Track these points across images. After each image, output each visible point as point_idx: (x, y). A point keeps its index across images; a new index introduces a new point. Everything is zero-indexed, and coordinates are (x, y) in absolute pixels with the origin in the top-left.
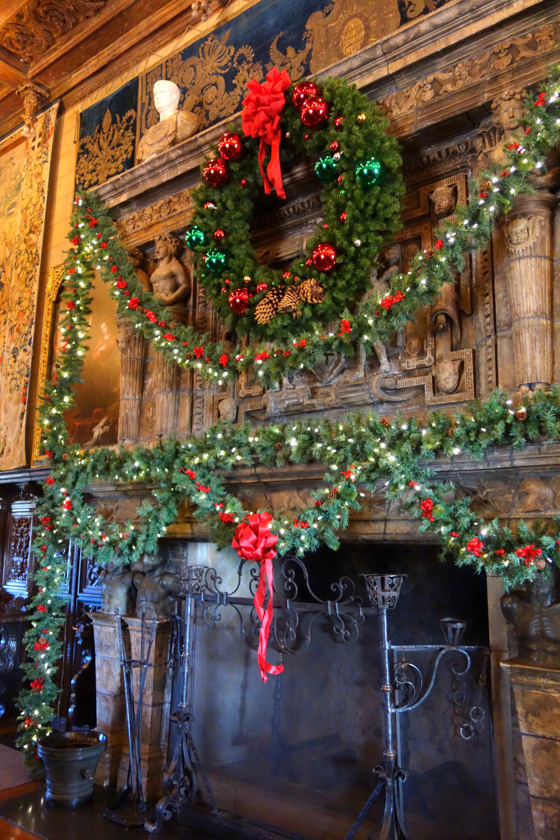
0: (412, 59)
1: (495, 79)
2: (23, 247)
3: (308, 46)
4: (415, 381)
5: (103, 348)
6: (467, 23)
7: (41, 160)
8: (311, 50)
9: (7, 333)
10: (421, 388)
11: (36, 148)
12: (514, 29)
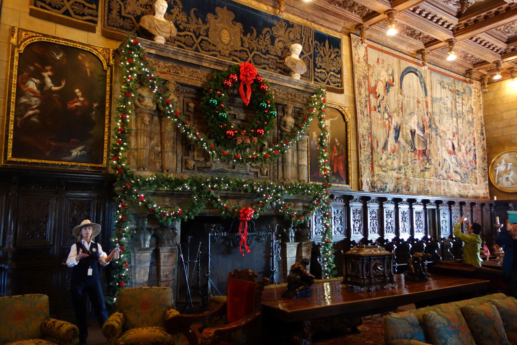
0: (274, 82)
1: (288, 100)
3: (208, 25)
4: (256, 170)
5: (78, 104)
6: (287, 83)
8: (209, 28)
10: (257, 173)
12: (292, 90)
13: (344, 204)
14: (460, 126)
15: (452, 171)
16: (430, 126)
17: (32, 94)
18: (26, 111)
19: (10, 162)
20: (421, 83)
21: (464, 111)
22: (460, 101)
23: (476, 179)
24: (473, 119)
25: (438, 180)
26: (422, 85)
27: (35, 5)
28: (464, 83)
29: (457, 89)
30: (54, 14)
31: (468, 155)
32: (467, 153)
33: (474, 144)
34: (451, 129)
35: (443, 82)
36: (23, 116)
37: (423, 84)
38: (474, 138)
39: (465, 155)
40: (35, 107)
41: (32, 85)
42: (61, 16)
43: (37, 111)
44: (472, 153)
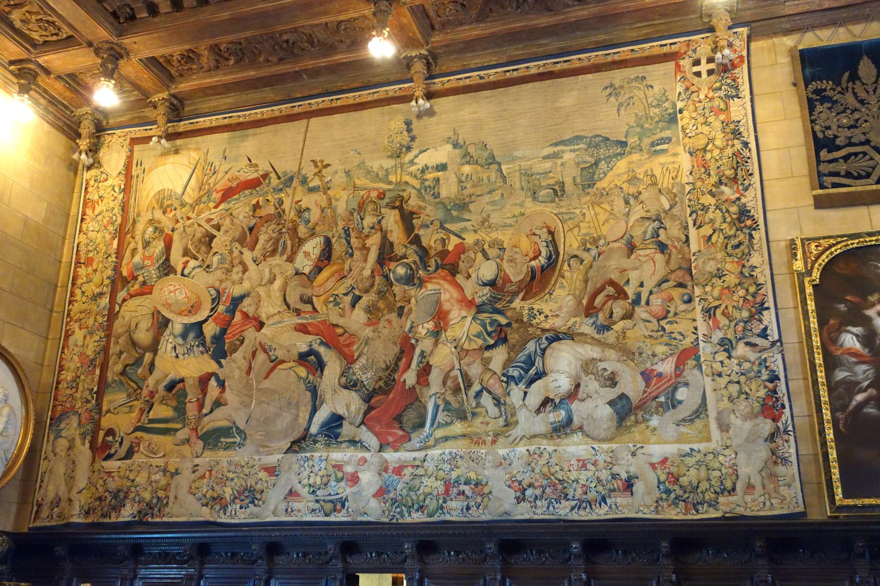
2: (708, 200)
7: (722, 93)
9: (699, 315)
11: (704, 75)
17: (854, 360)
18: (851, 400)
19: (842, 508)
27: (822, 187)
30: (859, 189)
36: (847, 406)
40: (866, 383)
41: (850, 340)
42: (874, 187)
43: (872, 391)
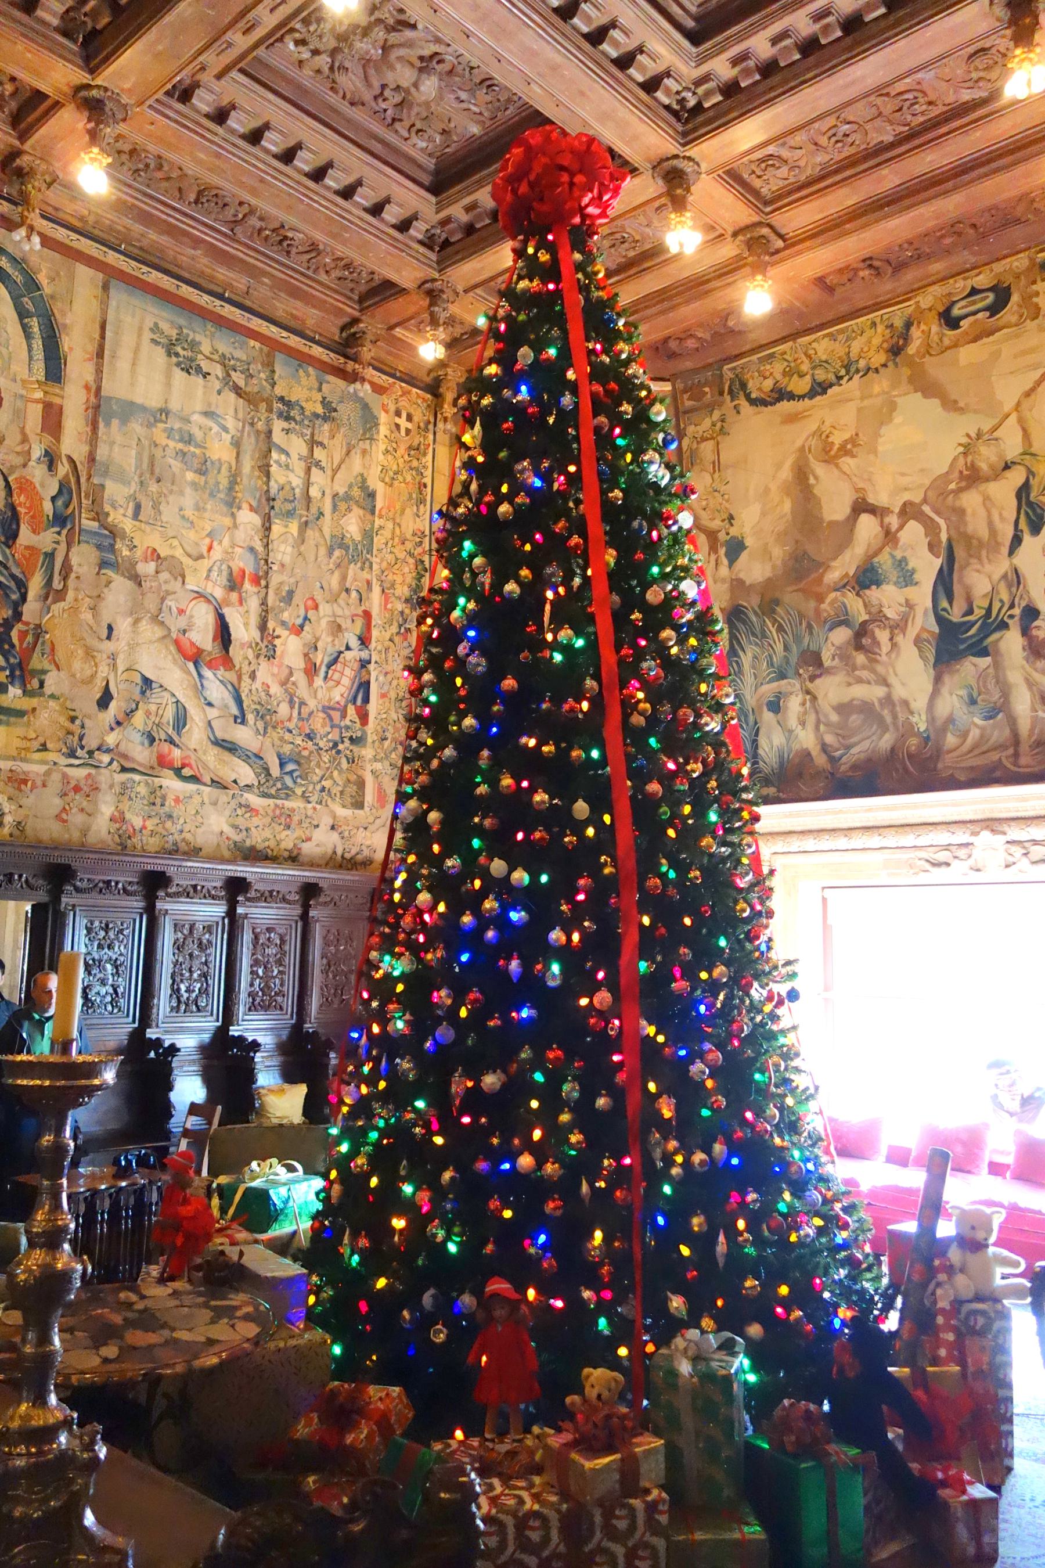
13: (142, 904)
14: (283, 552)
15: (195, 735)
16: (60, 520)
20: (22, 314)
21: (314, 492)
22: (297, 446)
23: (361, 784)
24: (368, 535)
25: (79, 774)
26: (26, 329)
28: (330, 378)
29: (279, 391)
31: (319, 681)
32: (311, 670)
33: (364, 641)
34: (217, 554)
35: (194, 345)
37: (34, 323)
38: (367, 615)
39: (299, 677)
44: (346, 677)
